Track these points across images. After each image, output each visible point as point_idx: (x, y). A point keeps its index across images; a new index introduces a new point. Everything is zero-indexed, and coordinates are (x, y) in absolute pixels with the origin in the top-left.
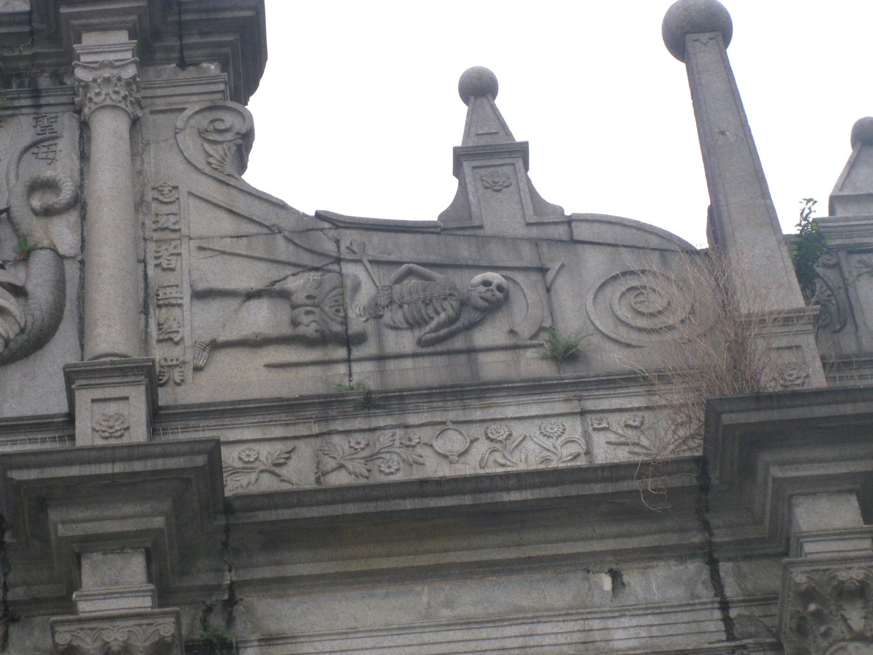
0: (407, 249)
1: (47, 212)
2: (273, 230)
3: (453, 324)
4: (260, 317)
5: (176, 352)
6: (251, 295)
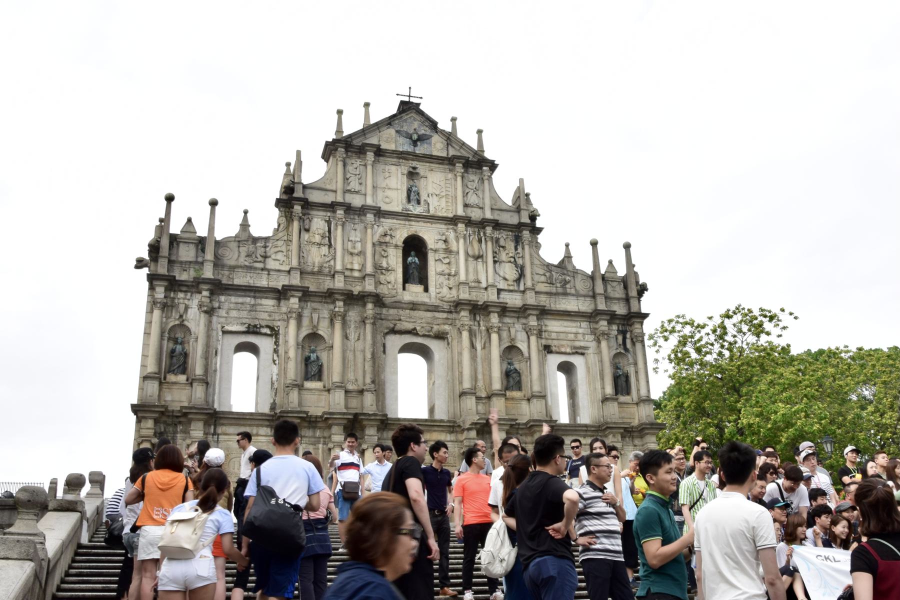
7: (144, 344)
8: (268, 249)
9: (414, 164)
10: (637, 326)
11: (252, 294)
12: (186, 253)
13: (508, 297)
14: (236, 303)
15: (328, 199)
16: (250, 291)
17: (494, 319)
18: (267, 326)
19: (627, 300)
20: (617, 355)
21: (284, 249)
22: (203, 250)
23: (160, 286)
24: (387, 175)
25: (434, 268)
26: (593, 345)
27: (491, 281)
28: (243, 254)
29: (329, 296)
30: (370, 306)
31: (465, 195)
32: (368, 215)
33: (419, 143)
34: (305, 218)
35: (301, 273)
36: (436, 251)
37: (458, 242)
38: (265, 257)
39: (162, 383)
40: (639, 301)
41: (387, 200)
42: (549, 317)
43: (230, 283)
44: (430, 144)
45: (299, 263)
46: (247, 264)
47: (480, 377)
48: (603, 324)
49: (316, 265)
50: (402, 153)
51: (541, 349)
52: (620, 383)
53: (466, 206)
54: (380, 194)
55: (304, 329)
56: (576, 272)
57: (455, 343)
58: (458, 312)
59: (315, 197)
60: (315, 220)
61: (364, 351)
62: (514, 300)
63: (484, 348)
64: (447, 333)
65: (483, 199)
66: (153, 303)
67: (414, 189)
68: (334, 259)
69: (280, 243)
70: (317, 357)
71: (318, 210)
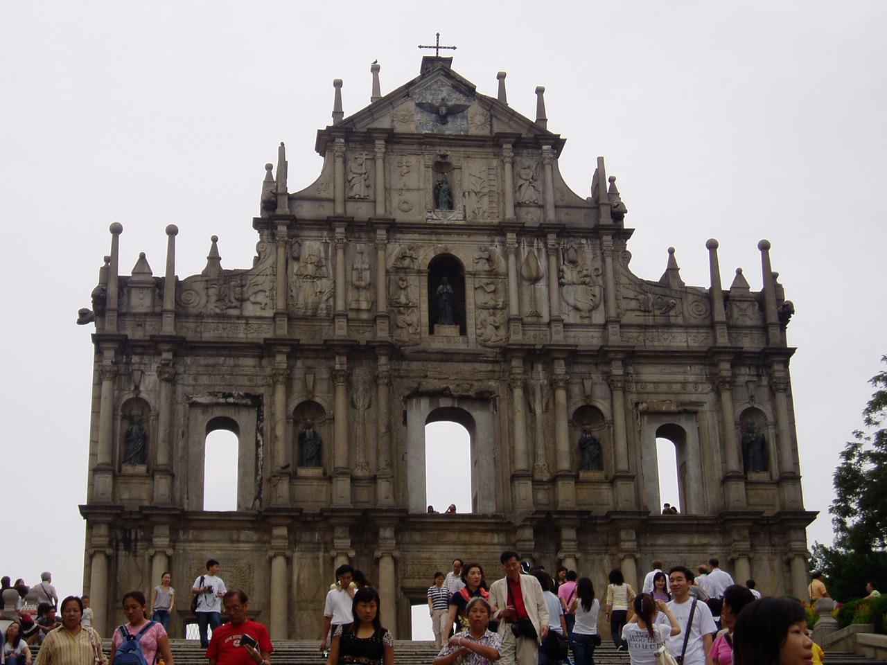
1: (597, 276)
2: (636, 284)
4: (634, 304)
5: (620, 311)
7: (92, 426)
8: (245, 289)
9: (443, 150)
10: (778, 367)
11: (225, 352)
12: (141, 302)
13: (582, 335)
14: (207, 366)
15: (326, 211)
16: (223, 348)
17: (560, 369)
18: (247, 396)
19: (764, 328)
20: (747, 413)
21: (267, 286)
22: (161, 297)
23: (109, 349)
25: (473, 298)
26: (709, 398)
27: (555, 313)
28: (214, 298)
29: (328, 349)
30: (383, 360)
31: (517, 189)
32: (379, 232)
33: (450, 119)
34: (293, 241)
35: (290, 319)
36: (474, 275)
37: (507, 259)
38: (242, 300)
39: (117, 476)
40: (783, 329)
41: (405, 207)
43: (198, 339)
44: (466, 118)
45: (287, 305)
46: (218, 311)
47: (540, 451)
48: (725, 368)
50: (426, 136)
51: (630, 407)
53: (518, 205)
54: (396, 199)
56: (685, 291)
57: (503, 406)
58: (508, 362)
59: (305, 211)
60: (307, 243)
61: (376, 423)
62: (588, 339)
63: (546, 410)
64: (491, 393)
65: (544, 193)
66: (100, 375)
67: (445, 186)
68: (333, 295)
69: (260, 279)
70: (314, 432)
71: (311, 229)
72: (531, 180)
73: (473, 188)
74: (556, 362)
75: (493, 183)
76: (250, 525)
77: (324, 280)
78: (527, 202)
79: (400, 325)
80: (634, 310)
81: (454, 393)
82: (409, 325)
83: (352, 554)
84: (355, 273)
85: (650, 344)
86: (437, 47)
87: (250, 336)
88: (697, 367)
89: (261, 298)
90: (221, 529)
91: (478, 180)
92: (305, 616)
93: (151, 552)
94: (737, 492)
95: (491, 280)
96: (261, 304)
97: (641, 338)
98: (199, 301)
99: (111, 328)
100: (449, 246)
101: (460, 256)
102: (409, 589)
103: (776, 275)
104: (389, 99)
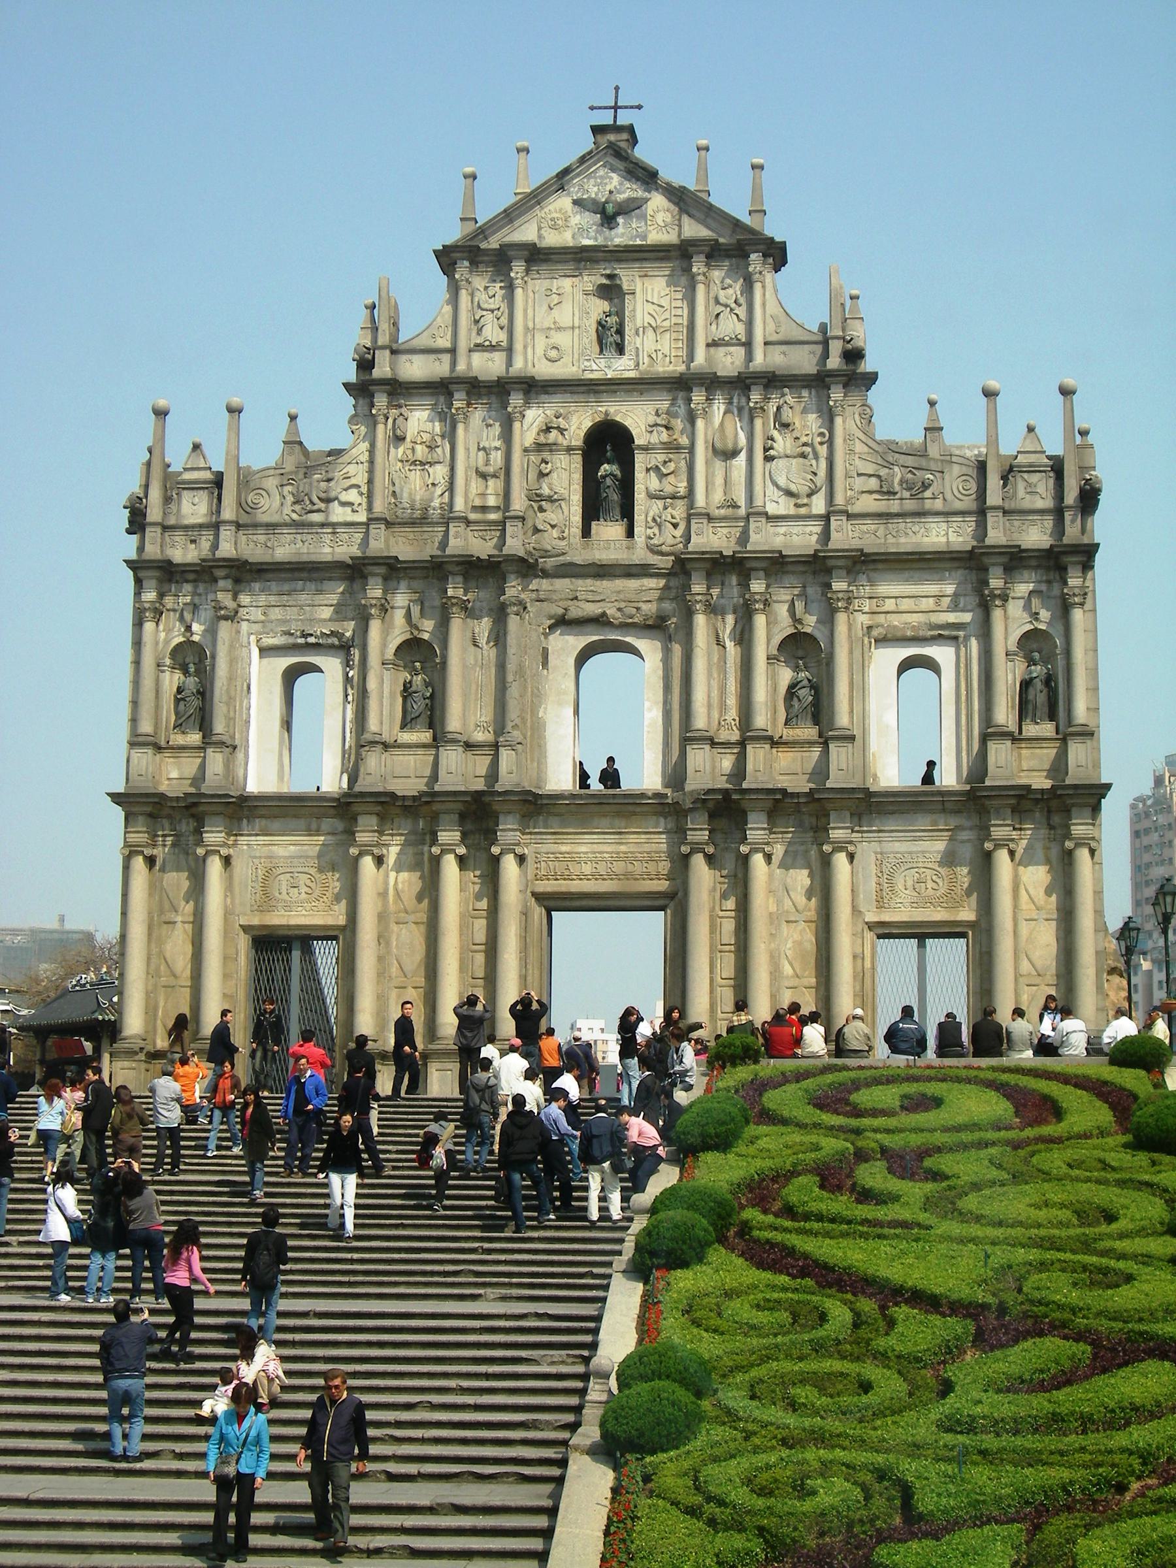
0: (910, 461)
1: (821, 443)
3: (918, 489)
4: (873, 483)
6: (871, 476)
8: (332, 484)
11: (304, 575)
13: (795, 530)
15: (438, 368)
17: (757, 586)
20: (1026, 636)
23: (151, 578)
24: (556, 299)
25: (644, 482)
33: (620, 220)
36: (646, 449)
38: (328, 501)
41: (553, 354)
42: (880, 566)
43: (268, 559)
44: (644, 217)
46: (295, 516)
49: (418, 506)
50: (585, 249)
51: (860, 634)
52: (1031, 697)
54: (541, 343)
55: (397, 631)
56: (948, 458)
58: (688, 574)
59: (415, 369)
69: (351, 469)
71: (422, 395)
72: (733, 305)
73: (648, 319)
74: (753, 574)
75: (679, 312)
76: (332, 811)
77: (438, 467)
78: (727, 338)
79: (540, 527)
80: (870, 492)
81: (615, 622)
82: (553, 527)
83: (462, 850)
84: (481, 453)
85: (892, 540)
86: (616, 108)
87: (338, 550)
88: (960, 572)
89: (352, 496)
90: (296, 816)
91: (658, 308)
92: (404, 931)
93: (200, 851)
94: (999, 752)
95: (671, 456)
96: (351, 504)
97: (880, 533)
98: (273, 505)
99: (153, 551)
100: (612, 410)
101: (628, 423)
102: (542, 894)
103: (1084, 433)
104: (535, 197)
